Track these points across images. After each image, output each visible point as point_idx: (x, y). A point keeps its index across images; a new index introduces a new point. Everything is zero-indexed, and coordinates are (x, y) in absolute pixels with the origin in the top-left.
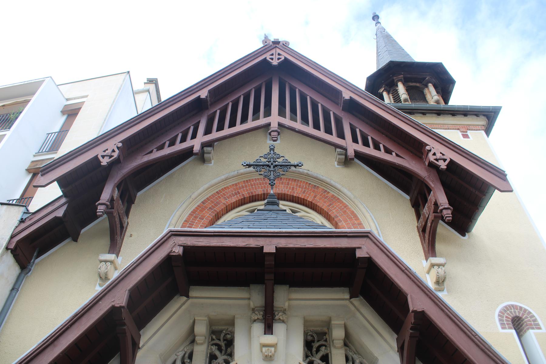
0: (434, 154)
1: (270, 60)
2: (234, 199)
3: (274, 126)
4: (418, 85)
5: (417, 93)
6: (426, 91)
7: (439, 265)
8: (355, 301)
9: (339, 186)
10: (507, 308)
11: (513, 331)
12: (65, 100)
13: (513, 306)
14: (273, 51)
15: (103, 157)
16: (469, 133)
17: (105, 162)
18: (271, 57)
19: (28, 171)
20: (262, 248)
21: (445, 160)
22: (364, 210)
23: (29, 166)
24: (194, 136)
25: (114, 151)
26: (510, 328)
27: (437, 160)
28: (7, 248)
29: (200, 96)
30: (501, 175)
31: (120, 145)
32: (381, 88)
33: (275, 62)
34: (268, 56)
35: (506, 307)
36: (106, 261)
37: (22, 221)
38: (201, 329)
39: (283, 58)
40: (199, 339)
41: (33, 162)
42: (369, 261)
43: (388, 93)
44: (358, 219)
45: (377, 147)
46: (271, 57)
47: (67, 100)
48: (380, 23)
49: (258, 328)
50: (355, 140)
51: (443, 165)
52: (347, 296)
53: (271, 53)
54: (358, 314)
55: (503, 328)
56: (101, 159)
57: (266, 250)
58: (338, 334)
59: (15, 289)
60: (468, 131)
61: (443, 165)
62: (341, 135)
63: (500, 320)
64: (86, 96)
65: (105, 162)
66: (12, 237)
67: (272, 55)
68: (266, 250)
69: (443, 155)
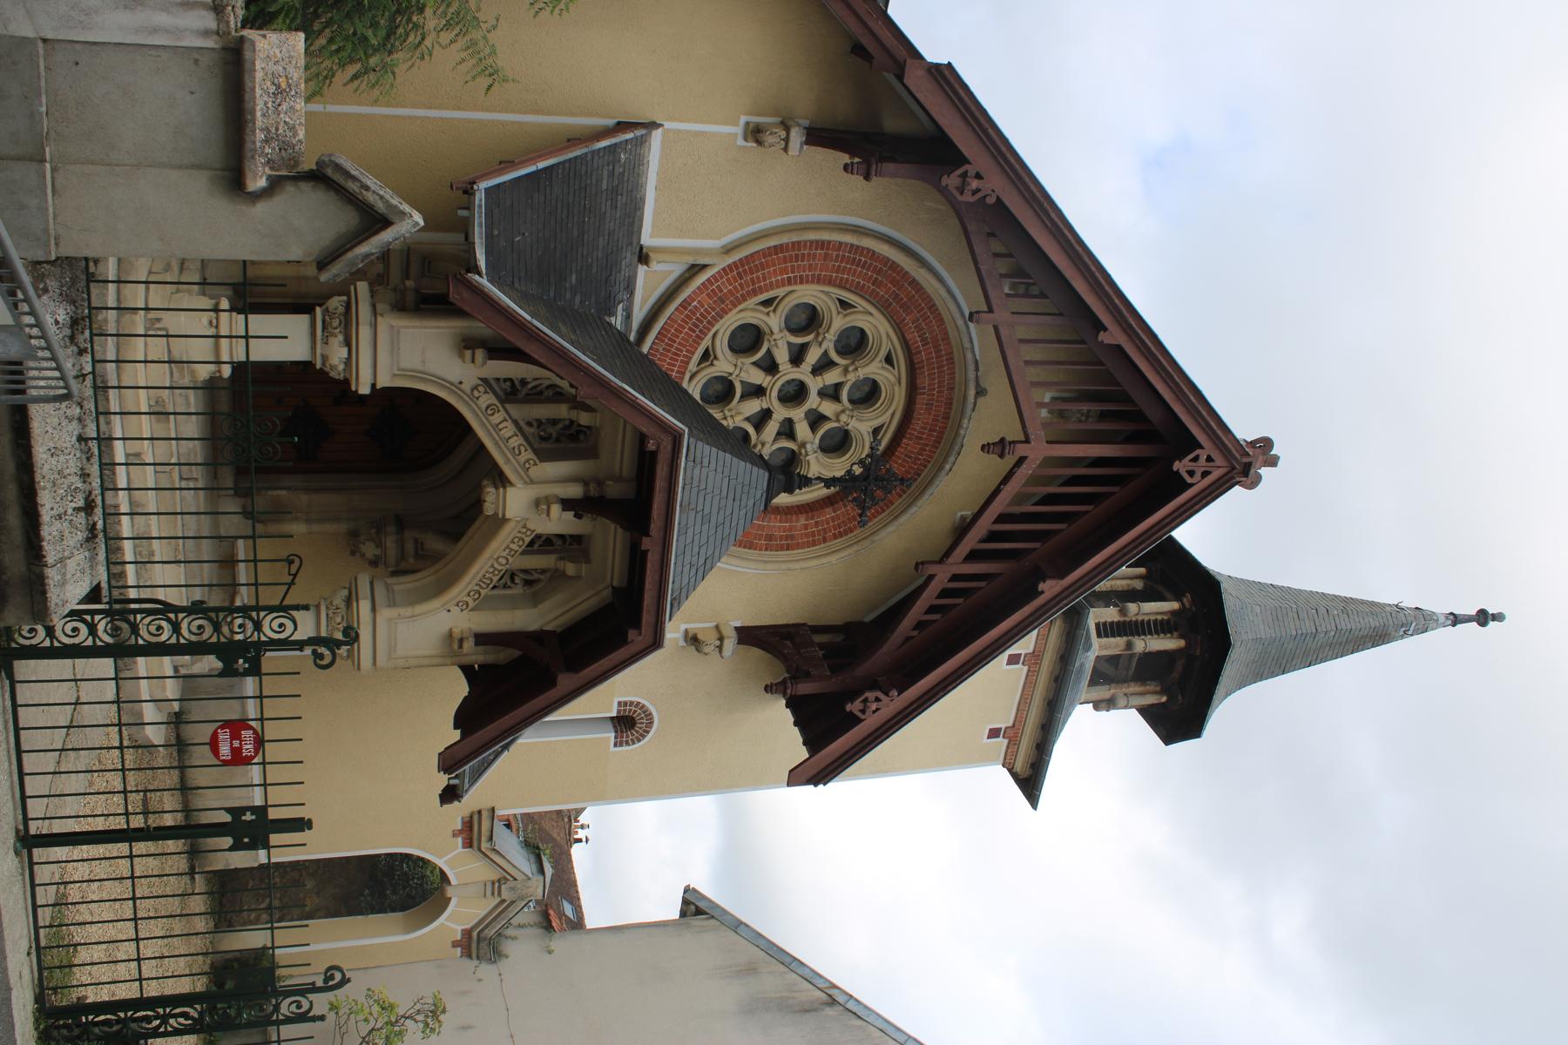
0: (877, 700)
1: (1191, 456)
2: (913, 336)
3: (1021, 450)
4: (1176, 675)
5: (1149, 669)
6: (1152, 687)
7: (720, 648)
8: (607, 593)
9: (903, 519)
10: (649, 715)
14: (1219, 460)
15: (965, 174)
16: (1001, 742)
20: (648, 535)
21: (863, 711)
22: (833, 559)
27: (866, 700)
29: (1106, 329)
30: (820, 776)
31: (991, 200)
32: (1193, 602)
34: (1208, 448)
38: (584, 419)
39: (1189, 480)
40: (574, 415)
42: (624, 641)
43: (1173, 613)
44: (835, 537)
45: (932, 609)
48: (1454, 625)
49: (574, 491)
50: (955, 578)
51: (854, 707)
52: (615, 584)
53: (1216, 455)
54: (591, 592)
56: (959, 172)
57: (645, 540)
58: (570, 569)
60: (1006, 741)
61: (854, 707)
62: (973, 556)
63: (632, 703)
68: (645, 540)
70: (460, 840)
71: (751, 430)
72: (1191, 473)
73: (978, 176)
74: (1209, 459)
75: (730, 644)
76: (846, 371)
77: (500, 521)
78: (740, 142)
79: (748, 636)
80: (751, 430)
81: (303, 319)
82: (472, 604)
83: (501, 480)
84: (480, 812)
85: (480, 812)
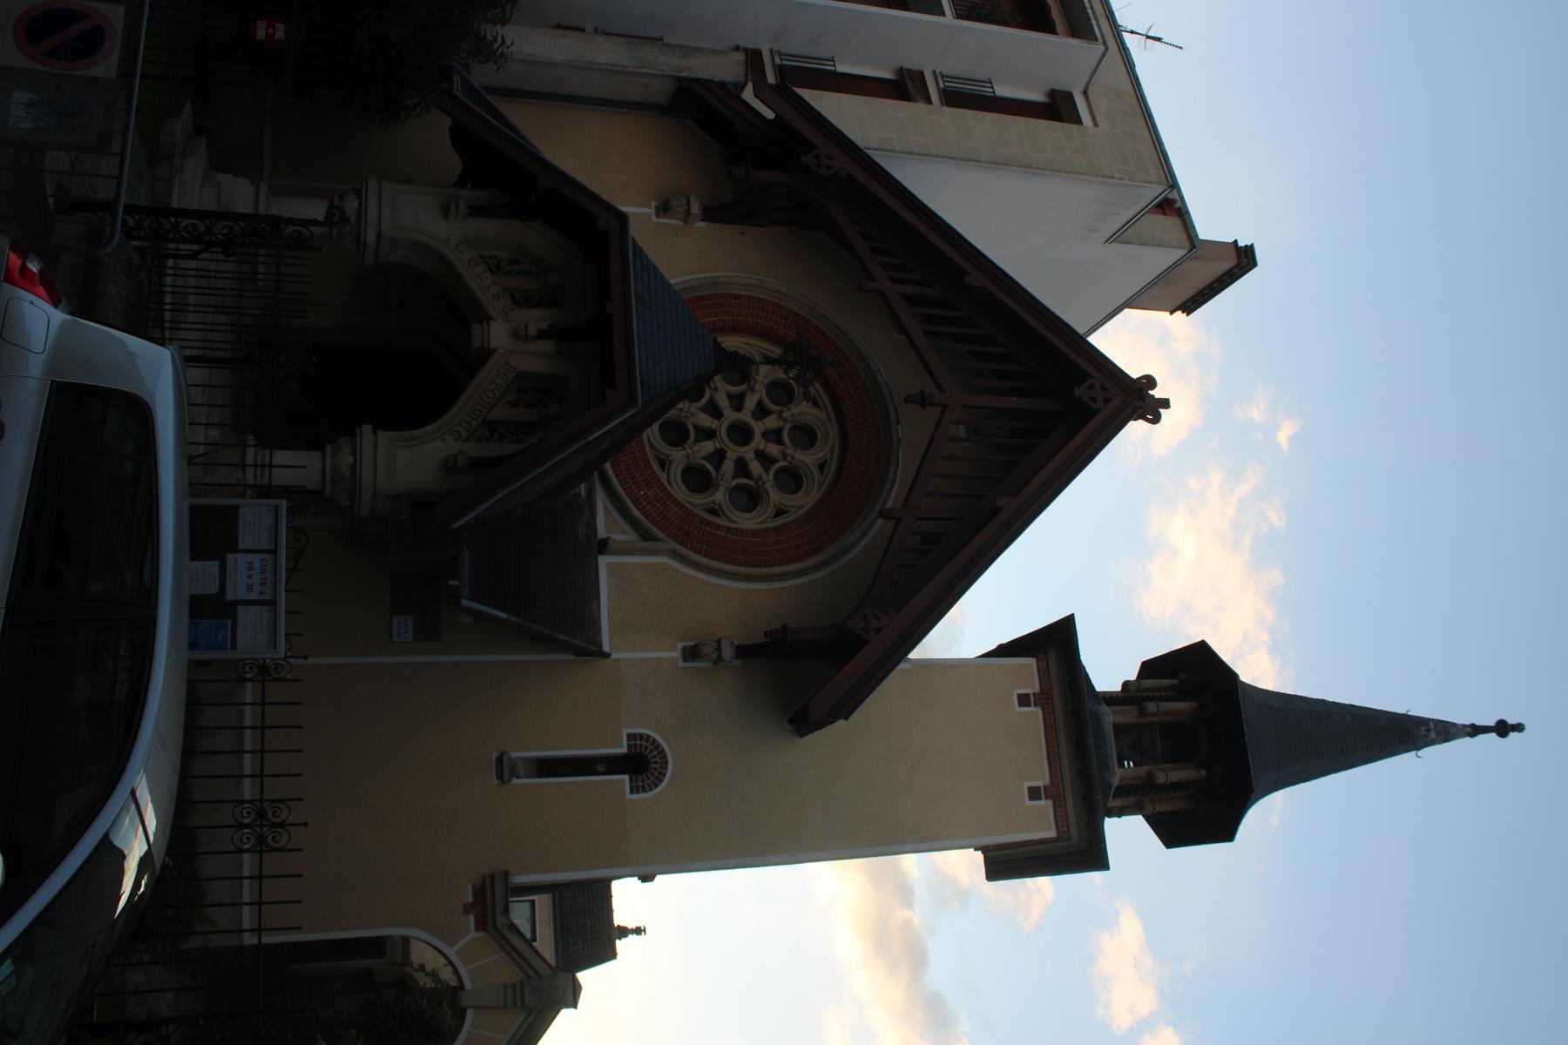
1: (1087, 384)
11: (624, 750)
12: (1081, 87)
13: (666, 762)
15: (817, 156)
16: (1045, 804)
17: (807, 160)
18: (1098, 387)
19: (901, 71)
23: (910, 71)
24: (894, 280)
25: (829, 168)
26: (629, 747)
28: (680, 79)
33: (1081, 392)
35: (663, 751)
36: (688, 204)
37: (722, 85)
41: (921, 74)
46: (1098, 387)
47: (1085, 93)
55: (629, 736)
59: (638, 106)
63: (641, 736)
64: (1096, 125)
65: (807, 160)
66: (697, 81)
67: (1104, 388)
69: (878, 630)
70: (472, 918)
71: (709, 466)
72: (1094, 400)
73: (830, 158)
74: (1104, 388)
75: (727, 653)
76: (781, 412)
77: (486, 354)
78: (654, 219)
79: (742, 651)
80: (709, 466)
81: (316, 455)
82: (464, 435)
83: (486, 318)
84: (492, 876)
85: (492, 876)
